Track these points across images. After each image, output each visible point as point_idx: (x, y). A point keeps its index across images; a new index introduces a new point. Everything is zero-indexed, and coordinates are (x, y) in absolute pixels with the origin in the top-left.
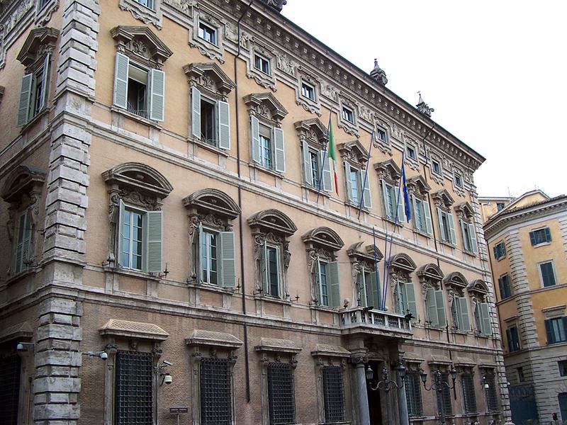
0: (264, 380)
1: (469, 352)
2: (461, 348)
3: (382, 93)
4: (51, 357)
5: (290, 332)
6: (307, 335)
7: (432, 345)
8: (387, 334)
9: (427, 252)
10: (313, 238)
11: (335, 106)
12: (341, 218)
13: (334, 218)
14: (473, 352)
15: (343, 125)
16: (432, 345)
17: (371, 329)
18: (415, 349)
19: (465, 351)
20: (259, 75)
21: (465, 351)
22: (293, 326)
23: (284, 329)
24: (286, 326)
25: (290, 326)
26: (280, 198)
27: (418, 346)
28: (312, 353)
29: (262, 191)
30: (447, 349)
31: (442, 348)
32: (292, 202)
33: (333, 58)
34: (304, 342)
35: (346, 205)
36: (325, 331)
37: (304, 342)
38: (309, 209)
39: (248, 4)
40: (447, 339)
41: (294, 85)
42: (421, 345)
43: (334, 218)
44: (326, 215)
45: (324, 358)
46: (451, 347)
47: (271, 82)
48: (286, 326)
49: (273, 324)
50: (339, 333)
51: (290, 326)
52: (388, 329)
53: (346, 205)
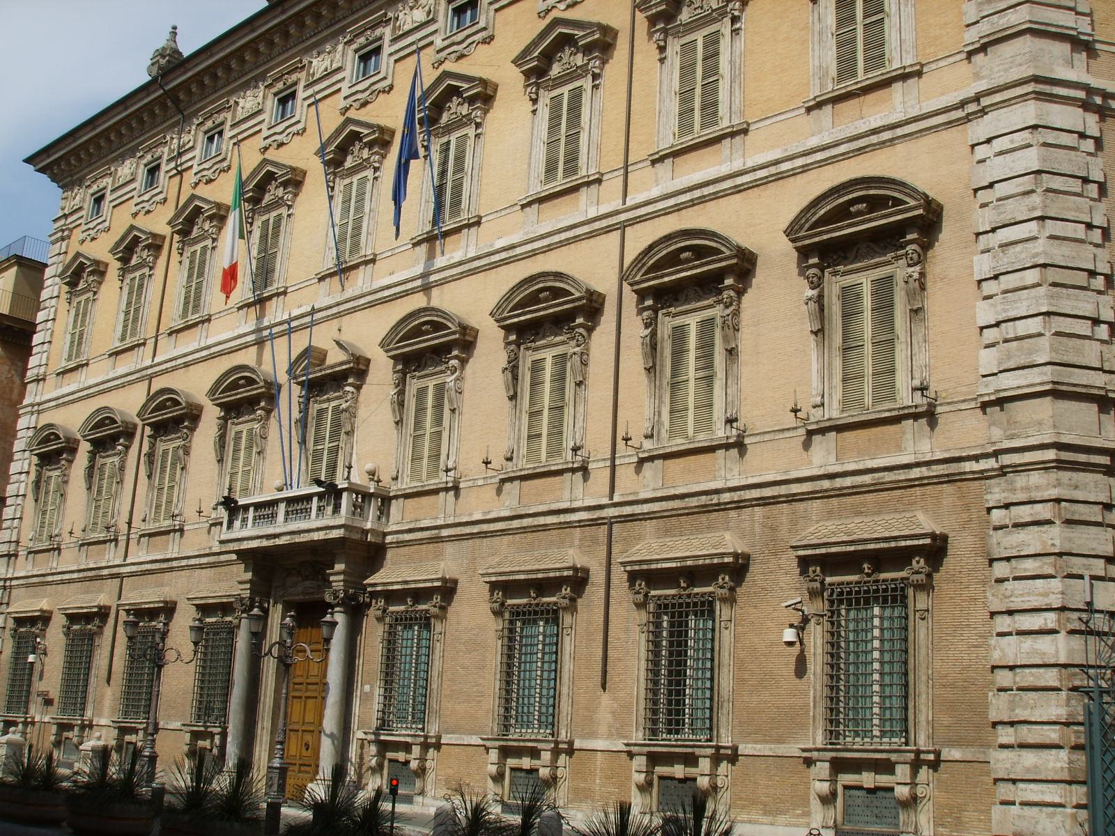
1: (721, 508)
3: (284, 17)
4: (1092, 627)
7: (516, 524)
9: (564, 236)
14: (764, 502)
16: (516, 524)
18: (449, 548)
19: (705, 510)
21: (705, 510)
27: (451, 539)
30: (594, 523)
31: (569, 525)
33: (197, 65)
39: (161, 91)
49: (149, 567)
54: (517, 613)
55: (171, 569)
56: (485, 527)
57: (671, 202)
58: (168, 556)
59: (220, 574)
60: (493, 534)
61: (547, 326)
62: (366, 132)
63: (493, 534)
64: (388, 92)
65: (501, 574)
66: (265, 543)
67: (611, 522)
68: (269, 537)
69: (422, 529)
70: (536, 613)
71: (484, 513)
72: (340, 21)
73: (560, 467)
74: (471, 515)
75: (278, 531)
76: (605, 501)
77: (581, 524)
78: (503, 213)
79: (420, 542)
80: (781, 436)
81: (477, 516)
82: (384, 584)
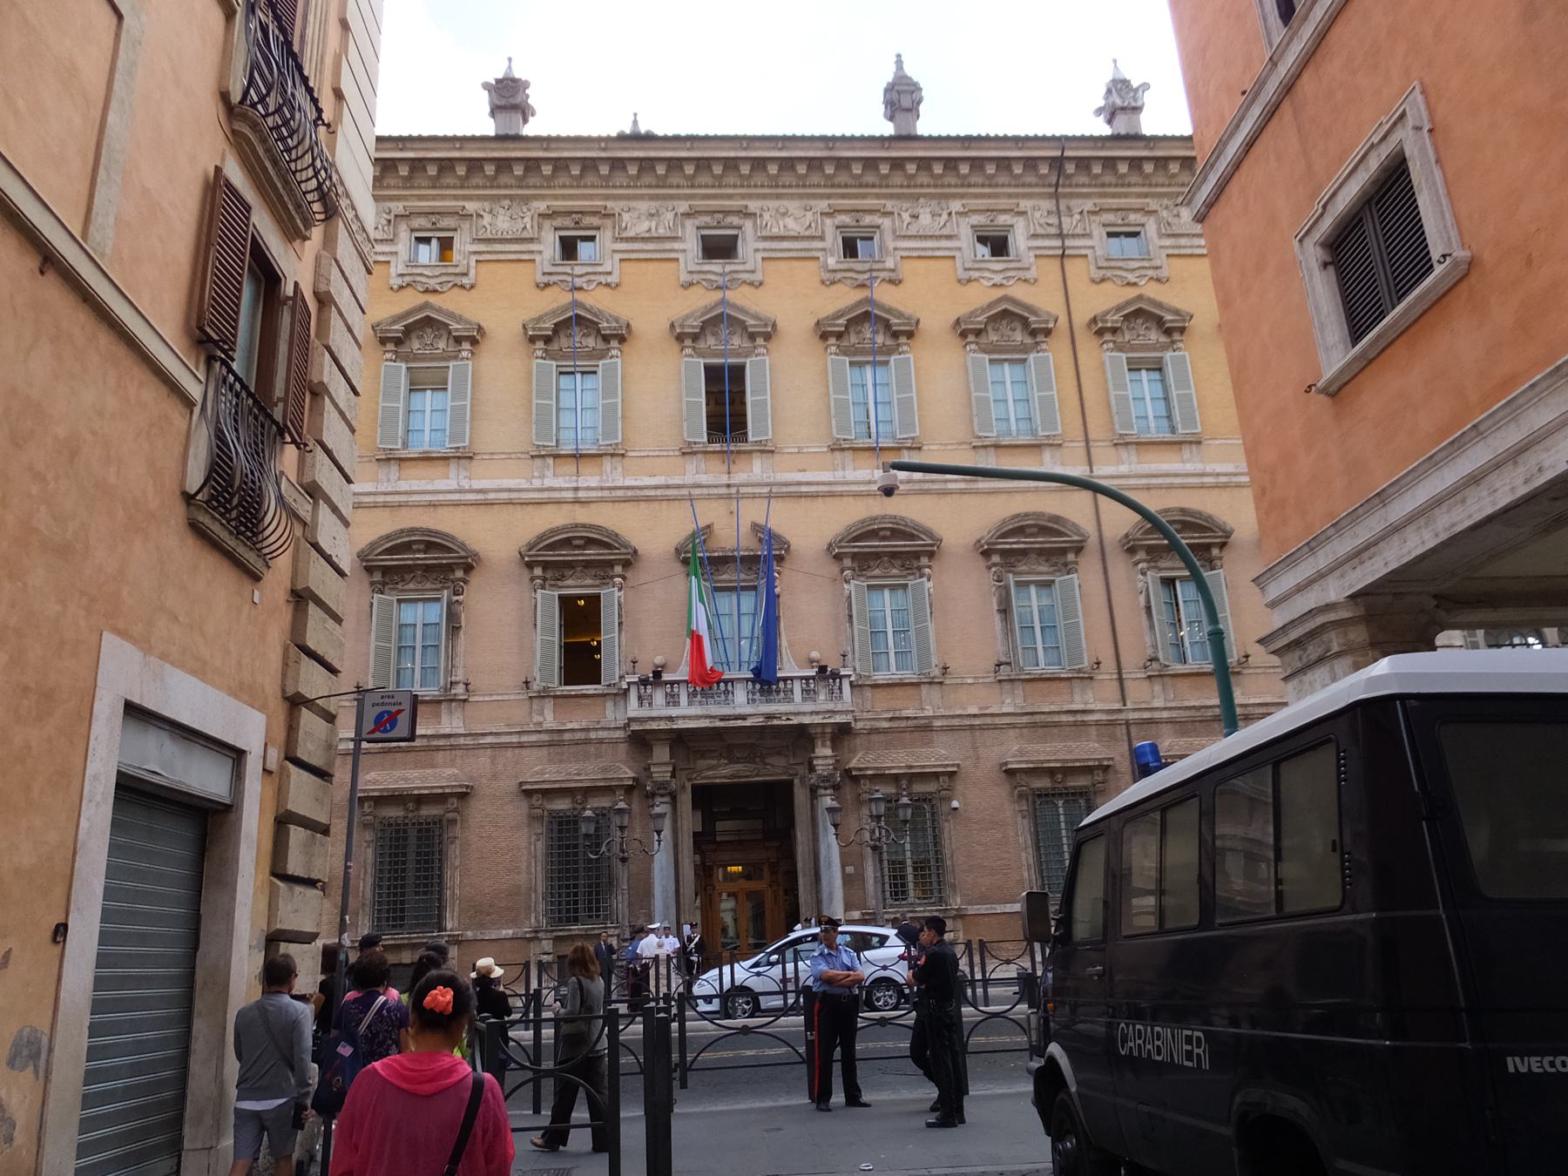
0: (370, 851)
2: (1188, 713)
5: (458, 752)
6: (509, 753)
8: (740, 723)
10: (530, 556)
11: (668, 246)
12: (656, 487)
13: (630, 493)
15: (696, 278)
16: (1025, 719)
17: (670, 719)
20: (421, 275)
22: (462, 741)
23: (438, 749)
24: (441, 742)
25: (453, 741)
26: (456, 497)
27: (943, 729)
28: (521, 784)
29: (403, 498)
30: (1112, 723)
31: (1084, 724)
32: (491, 496)
34: (500, 767)
35: (684, 454)
36: (567, 736)
37: (500, 767)
38: (546, 495)
40: (1118, 695)
41: (532, 252)
42: (975, 727)
43: (630, 493)
44: (606, 494)
45: (547, 793)
46: (1136, 715)
47: (456, 274)
48: (441, 742)
50: (619, 734)
51: (453, 741)
52: (748, 710)
53: (684, 454)
54: (1041, 795)
55: (453, 748)
56: (997, 720)
57: (1143, 481)
58: (442, 731)
59: (563, 754)
60: (995, 727)
61: (1033, 556)
62: (752, 322)
63: (995, 727)
64: (757, 287)
65: (1032, 762)
66: (719, 724)
67: (1127, 723)
68: (723, 718)
69: (908, 718)
70: (1053, 795)
71: (981, 708)
72: (671, 187)
73: (1070, 675)
74: (965, 709)
75: (739, 711)
76: (1117, 706)
77: (1097, 723)
78: (949, 447)
79: (903, 731)
80: (1272, 671)
81: (973, 710)
82: (860, 769)
